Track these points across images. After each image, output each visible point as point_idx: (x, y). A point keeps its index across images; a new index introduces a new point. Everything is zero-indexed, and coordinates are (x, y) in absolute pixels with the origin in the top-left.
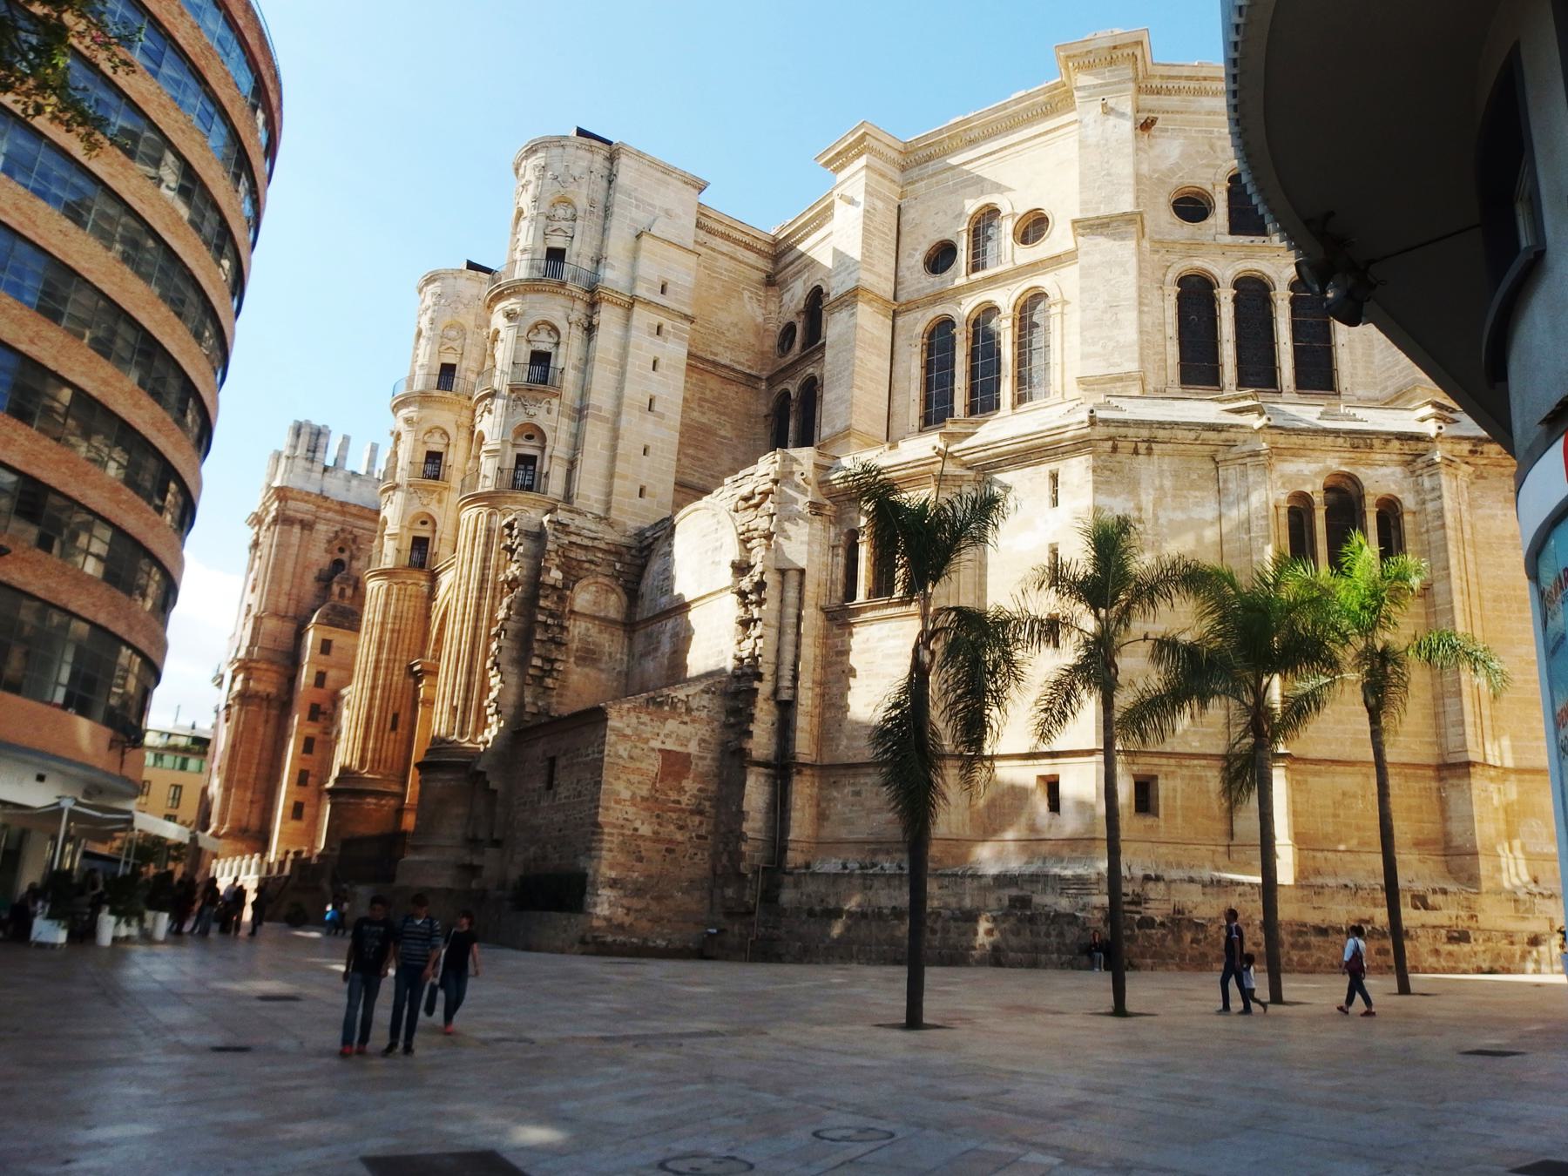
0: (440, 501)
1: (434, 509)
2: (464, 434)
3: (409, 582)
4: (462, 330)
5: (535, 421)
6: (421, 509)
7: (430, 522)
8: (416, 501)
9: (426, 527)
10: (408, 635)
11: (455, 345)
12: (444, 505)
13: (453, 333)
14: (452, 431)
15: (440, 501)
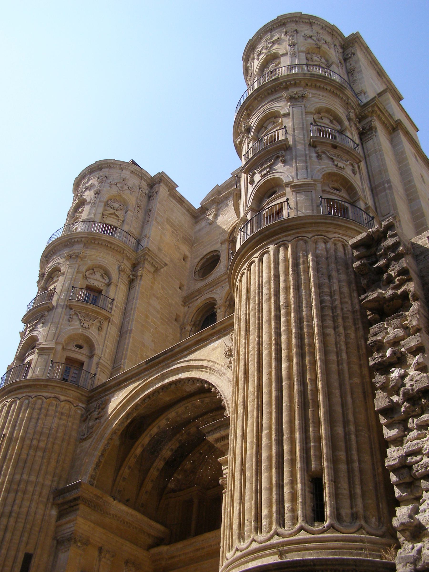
0: (100, 329)
1: (93, 333)
2: (125, 279)
3: (62, 398)
4: (124, 204)
5: (343, 173)
6: (81, 331)
7: (86, 347)
8: (76, 324)
9: (82, 351)
10: (54, 456)
11: (118, 213)
12: (103, 333)
13: (116, 205)
14: (114, 274)
15: (100, 329)
